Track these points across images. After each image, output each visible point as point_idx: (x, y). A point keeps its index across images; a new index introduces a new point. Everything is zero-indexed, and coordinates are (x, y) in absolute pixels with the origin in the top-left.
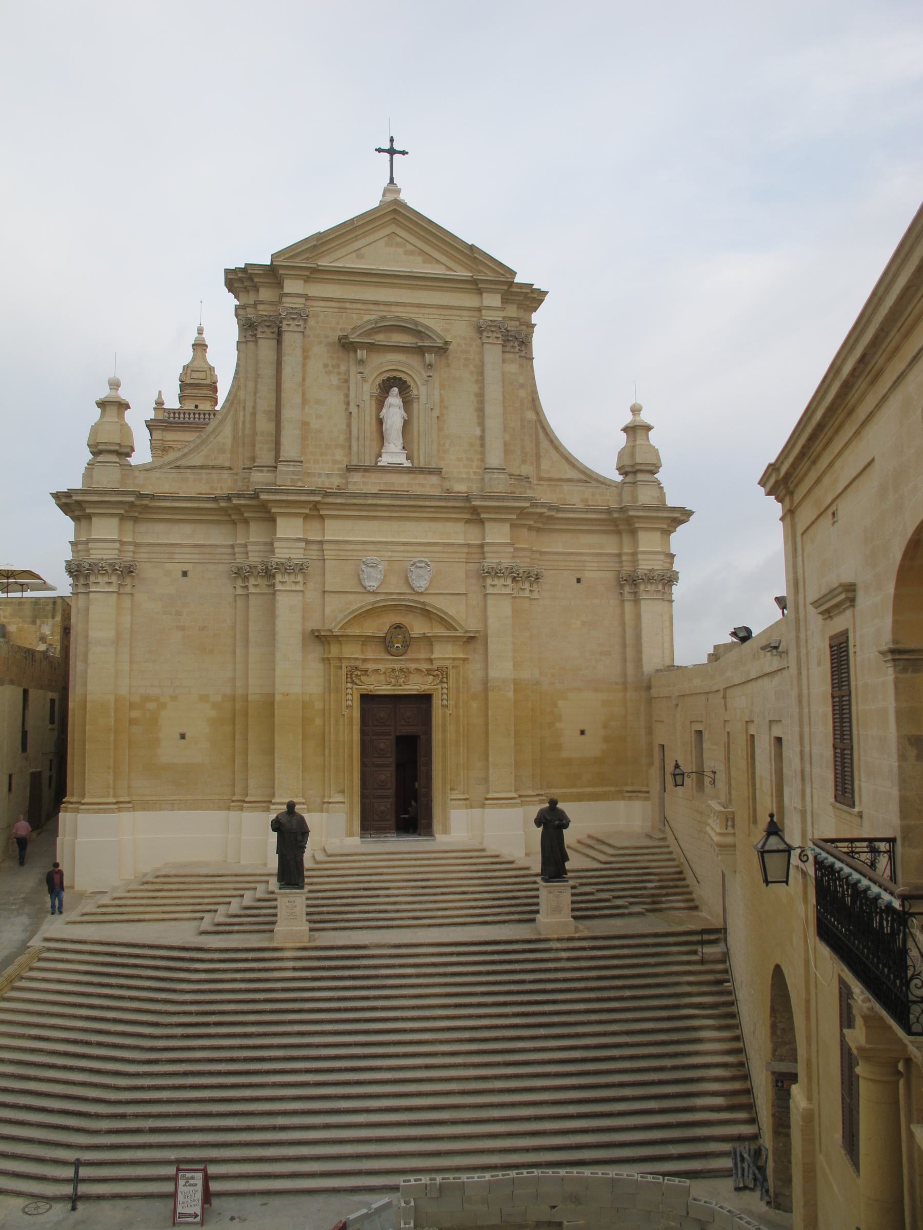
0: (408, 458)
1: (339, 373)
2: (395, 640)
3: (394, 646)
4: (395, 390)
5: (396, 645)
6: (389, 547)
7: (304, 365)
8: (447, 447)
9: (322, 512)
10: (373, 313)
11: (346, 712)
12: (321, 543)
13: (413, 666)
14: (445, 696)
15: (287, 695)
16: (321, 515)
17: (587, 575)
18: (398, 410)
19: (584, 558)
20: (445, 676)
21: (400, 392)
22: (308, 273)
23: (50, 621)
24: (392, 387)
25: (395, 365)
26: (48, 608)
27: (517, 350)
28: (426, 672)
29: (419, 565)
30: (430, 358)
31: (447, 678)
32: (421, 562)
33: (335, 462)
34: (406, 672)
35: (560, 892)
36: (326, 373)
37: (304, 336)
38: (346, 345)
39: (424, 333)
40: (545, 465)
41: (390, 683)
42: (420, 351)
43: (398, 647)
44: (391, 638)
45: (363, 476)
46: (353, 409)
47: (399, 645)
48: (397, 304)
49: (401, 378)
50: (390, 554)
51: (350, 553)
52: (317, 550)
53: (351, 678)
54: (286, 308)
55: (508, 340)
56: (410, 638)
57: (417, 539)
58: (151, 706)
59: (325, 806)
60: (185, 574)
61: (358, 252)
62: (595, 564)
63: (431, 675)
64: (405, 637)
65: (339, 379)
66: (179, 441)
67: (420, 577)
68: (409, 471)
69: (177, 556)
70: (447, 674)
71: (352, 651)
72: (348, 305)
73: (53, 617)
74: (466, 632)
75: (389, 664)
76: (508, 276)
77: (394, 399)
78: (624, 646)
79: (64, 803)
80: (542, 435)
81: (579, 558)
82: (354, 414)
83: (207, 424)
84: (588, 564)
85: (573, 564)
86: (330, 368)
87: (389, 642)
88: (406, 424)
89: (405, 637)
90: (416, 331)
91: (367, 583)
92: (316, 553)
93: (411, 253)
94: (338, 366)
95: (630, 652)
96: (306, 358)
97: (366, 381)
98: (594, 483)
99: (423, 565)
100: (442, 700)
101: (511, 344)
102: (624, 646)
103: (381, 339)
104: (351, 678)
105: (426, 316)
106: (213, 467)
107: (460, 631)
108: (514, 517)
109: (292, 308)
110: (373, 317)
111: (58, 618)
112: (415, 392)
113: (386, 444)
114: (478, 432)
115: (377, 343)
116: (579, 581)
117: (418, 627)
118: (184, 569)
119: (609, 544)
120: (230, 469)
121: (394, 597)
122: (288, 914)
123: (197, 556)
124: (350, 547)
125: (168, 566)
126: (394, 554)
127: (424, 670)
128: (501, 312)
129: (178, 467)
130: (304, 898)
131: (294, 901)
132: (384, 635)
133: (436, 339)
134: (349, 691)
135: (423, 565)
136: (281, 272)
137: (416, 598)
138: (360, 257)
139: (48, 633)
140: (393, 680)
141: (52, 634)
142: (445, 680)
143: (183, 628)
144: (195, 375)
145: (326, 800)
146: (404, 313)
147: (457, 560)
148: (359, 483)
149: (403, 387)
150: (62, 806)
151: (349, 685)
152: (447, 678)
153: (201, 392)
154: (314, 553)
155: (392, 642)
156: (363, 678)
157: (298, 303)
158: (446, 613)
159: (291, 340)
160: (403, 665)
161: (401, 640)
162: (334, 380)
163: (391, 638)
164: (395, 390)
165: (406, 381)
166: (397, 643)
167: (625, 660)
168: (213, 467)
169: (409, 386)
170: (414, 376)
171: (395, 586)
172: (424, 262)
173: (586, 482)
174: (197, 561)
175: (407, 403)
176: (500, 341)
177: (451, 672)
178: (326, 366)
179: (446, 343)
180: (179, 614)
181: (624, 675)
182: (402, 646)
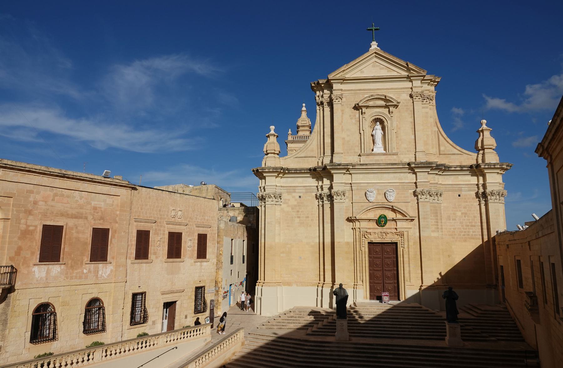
0: (385, 149)
1: (355, 119)
4: (378, 123)
6: (377, 184)
7: (342, 116)
8: (400, 144)
9: (351, 172)
10: (368, 94)
11: (363, 249)
12: (351, 184)
13: (389, 231)
14: (403, 243)
15: (339, 242)
16: (350, 173)
17: (463, 194)
18: (379, 131)
19: (461, 186)
20: (402, 235)
21: (380, 124)
22: (342, 81)
23: (252, 216)
24: (377, 122)
25: (377, 113)
26: (251, 210)
27: (428, 103)
29: (390, 191)
30: (391, 109)
31: (403, 236)
32: (391, 190)
33: (355, 152)
34: (386, 234)
36: (350, 118)
37: (342, 105)
38: (357, 108)
39: (389, 100)
40: (442, 148)
42: (386, 107)
45: (366, 157)
46: (362, 132)
48: (378, 89)
49: (380, 118)
50: (378, 187)
51: (362, 187)
52: (350, 187)
53: (364, 236)
54: (334, 95)
55: (424, 99)
57: (389, 180)
59: (355, 286)
60: (300, 197)
61: (361, 70)
62: (467, 189)
65: (356, 121)
66: (297, 147)
67: (390, 195)
68: (384, 154)
69: (297, 190)
70: (403, 235)
71: (364, 224)
72: (358, 92)
73: (253, 214)
74: (411, 217)
75: (380, 230)
76: (423, 73)
77: (378, 127)
79: (257, 282)
80: (440, 136)
81: (459, 186)
82: (362, 134)
83: (307, 140)
84: (463, 189)
85: (457, 189)
86: (352, 117)
88: (384, 135)
90: (386, 100)
91: (369, 199)
92: (349, 187)
93: (382, 69)
94: (355, 116)
96: (343, 113)
97: (366, 121)
98: (464, 154)
99: (392, 191)
100: (402, 245)
101: (425, 100)
102: (481, 223)
103: (371, 103)
104: (364, 236)
105: (389, 93)
106: (309, 157)
107: (408, 217)
108: (429, 170)
109: (337, 95)
110: (368, 95)
111: (255, 215)
112: (386, 123)
113: (375, 144)
114: (413, 137)
115: (370, 105)
116: (459, 196)
117: (390, 215)
118: (300, 195)
119: (473, 180)
120: (316, 157)
121: (380, 204)
123: (304, 190)
124: (362, 185)
125: (294, 194)
126: (380, 187)
128: (421, 88)
129: (296, 157)
130: (346, 322)
131: (343, 324)
132: (377, 219)
133: (394, 102)
134: (364, 241)
135: (392, 191)
136: (332, 81)
137: (390, 204)
138: (362, 72)
139: (251, 220)
140: (381, 237)
141: (253, 220)
142: (402, 237)
143: (299, 217)
144: (303, 122)
145: (356, 284)
146: (380, 92)
147: (405, 189)
148: (364, 160)
149: (382, 122)
150: (257, 284)
152: (403, 236)
153: (305, 128)
154: (348, 187)
157: (339, 93)
158: (402, 210)
159: (337, 107)
160: (385, 230)
162: (354, 121)
165: (382, 119)
168: (309, 157)
169: (384, 121)
170: (385, 117)
171: (381, 199)
172: (388, 72)
173: (461, 154)
174: (304, 192)
175: (383, 129)
176: (421, 100)
177: (405, 234)
178: (350, 116)
179: (398, 103)
180: (298, 211)
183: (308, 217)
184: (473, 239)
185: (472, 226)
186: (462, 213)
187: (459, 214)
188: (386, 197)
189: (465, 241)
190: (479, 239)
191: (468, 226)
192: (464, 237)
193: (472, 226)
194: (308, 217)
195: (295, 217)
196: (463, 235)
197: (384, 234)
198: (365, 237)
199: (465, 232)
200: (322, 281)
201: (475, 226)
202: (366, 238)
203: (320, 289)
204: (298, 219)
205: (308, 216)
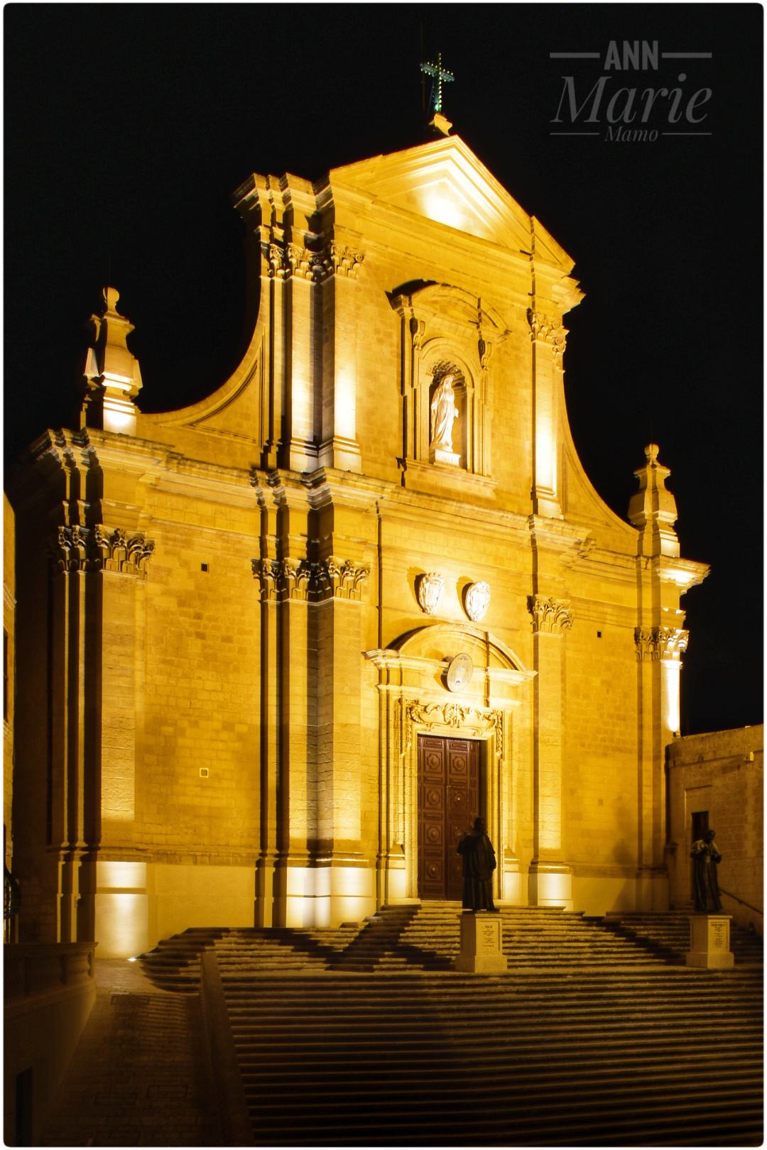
5: (457, 680)
15: (346, 725)
35: (721, 925)
43: (458, 682)
47: (460, 680)
58: (169, 730)
70: (501, 719)
78: (640, 711)
95: (648, 719)
102: (640, 711)
122: (485, 941)
151: (410, 722)
156: (424, 716)
164: (448, 382)
167: (641, 727)
181: (641, 742)
183: (228, 639)
184: (620, 750)
185: (619, 717)
186: (604, 682)
187: (596, 682)
188: (468, 606)
189: (605, 755)
190: (631, 752)
191: (611, 716)
192: (603, 743)
193: (619, 717)
194: (228, 639)
195: (189, 635)
196: (604, 740)
197: (458, 713)
198: (412, 718)
199: (606, 732)
200: (272, 849)
201: (624, 719)
202: (415, 721)
203: (269, 871)
204: (199, 642)
205: (229, 634)
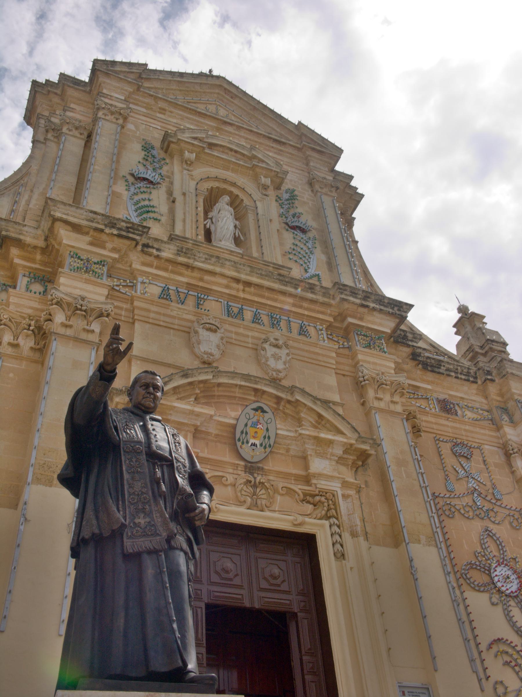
2: (251, 431)
3: (247, 442)
5: (252, 441)
20: (332, 507)
28: (302, 496)
41: (241, 503)
43: (254, 445)
44: (246, 425)
47: (257, 442)
56: (276, 434)
63: (308, 502)
64: (267, 430)
70: (334, 504)
87: (242, 432)
89: (267, 430)
127: (297, 490)
132: (233, 422)
155: (247, 433)
161: (261, 433)
163: (246, 425)
166: (254, 437)
182: (261, 445)
